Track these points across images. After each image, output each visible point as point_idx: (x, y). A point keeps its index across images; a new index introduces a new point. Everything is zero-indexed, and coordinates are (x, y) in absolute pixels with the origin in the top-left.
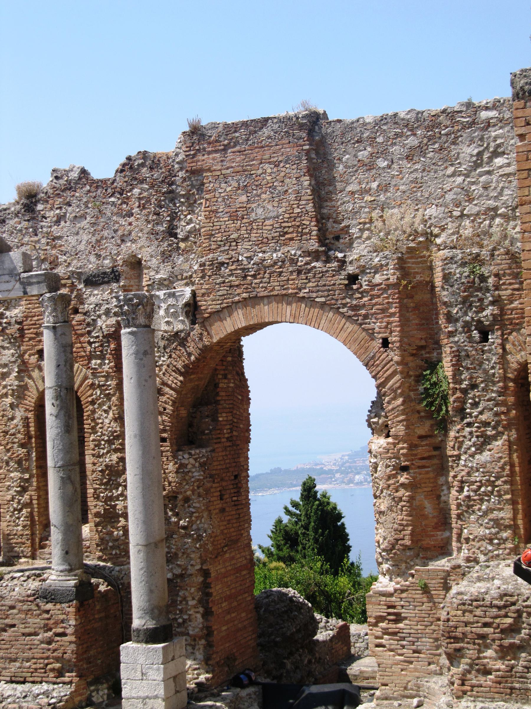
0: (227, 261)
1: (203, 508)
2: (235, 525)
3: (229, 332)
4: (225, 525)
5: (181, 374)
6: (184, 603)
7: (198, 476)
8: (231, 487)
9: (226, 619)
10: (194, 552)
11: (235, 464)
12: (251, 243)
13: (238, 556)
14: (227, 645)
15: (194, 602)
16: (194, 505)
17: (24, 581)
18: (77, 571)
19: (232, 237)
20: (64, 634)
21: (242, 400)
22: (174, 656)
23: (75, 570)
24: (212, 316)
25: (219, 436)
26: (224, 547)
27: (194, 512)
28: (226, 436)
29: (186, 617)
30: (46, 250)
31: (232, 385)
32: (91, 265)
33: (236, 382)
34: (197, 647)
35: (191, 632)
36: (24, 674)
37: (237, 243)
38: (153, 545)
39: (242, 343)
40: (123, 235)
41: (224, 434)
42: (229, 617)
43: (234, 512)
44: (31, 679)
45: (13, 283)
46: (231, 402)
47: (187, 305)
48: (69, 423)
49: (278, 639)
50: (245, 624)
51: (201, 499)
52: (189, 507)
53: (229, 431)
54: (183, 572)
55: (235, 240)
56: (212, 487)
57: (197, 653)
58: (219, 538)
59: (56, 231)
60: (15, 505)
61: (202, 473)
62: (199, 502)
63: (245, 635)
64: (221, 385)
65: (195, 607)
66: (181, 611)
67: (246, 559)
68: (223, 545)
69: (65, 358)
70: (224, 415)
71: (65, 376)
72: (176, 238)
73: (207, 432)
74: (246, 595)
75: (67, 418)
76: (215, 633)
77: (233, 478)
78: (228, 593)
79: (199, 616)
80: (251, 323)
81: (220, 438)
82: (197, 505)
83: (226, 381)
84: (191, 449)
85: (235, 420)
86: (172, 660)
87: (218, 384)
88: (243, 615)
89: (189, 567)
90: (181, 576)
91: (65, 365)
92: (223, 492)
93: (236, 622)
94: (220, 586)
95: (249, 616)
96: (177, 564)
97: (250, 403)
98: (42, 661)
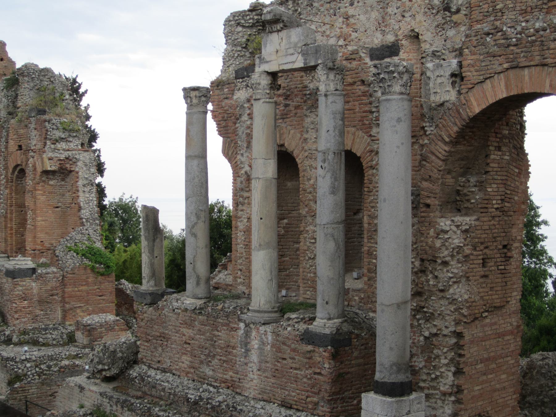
0: (493, 31)
1: (461, 274)
2: (500, 292)
3: (490, 103)
4: (487, 292)
5: (446, 143)
6: (437, 360)
7: (459, 243)
8: (498, 255)
9: (480, 379)
10: (449, 315)
11: (504, 234)
12: (515, 13)
13: (502, 322)
14: (480, 403)
15: (446, 361)
16: (452, 270)
17: (296, 322)
18: (336, 320)
19: (498, 7)
20: (319, 374)
21: (519, 173)
22: (409, 411)
23: (333, 319)
24: (476, 86)
25: (487, 206)
26: (483, 312)
27: (452, 278)
28: (496, 206)
29: (438, 374)
30: (342, 28)
31: (506, 157)
32: (377, 40)
33: (513, 155)
34: (446, 402)
35: (442, 389)
36: (291, 402)
37: (502, 13)
38: (395, 305)
39: (525, 118)
40: (404, 11)
41: (493, 204)
42: (485, 378)
43: (500, 280)
44: (295, 407)
45: (296, 55)
46: (506, 173)
47: (453, 75)
48: (334, 185)
49: (546, 400)
50: (504, 385)
51: (460, 265)
52: (448, 271)
53: (499, 202)
54: (438, 332)
55: (501, 10)
56: (472, 254)
57: (446, 408)
58: (478, 304)
59: (351, 11)
60: (309, 255)
61: (463, 240)
62: (457, 268)
63: (504, 395)
64: (492, 157)
65: (446, 365)
66: (434, 367)
67: (511, 325)
68: (483, 310)
69: (334, 124)
70: (495, 186)
71: (333, 141)
72: (450, 12)
73: (473, 201)
74: (509, 358)
75: (333, 180)
76: (465, 392)
77: (501, 247)
78: (485, 356)
79: (450, 374)
80: (512, 94)
81: (487, 208)
82: (456, 271)
83: (500, 153)
84: (454, 217)
85: (509, 192)
86: (407, 414)
87: (490, 155)
88: (504, 376)
89: (444, 328)
90: (436, 335)
91: (334, 131)
92: (487, 261)
93: (493, 383)
94: (476, 349)
95: (511, 378)
96: (434, 325)
97: (529, 177)
98: (303, 393)
